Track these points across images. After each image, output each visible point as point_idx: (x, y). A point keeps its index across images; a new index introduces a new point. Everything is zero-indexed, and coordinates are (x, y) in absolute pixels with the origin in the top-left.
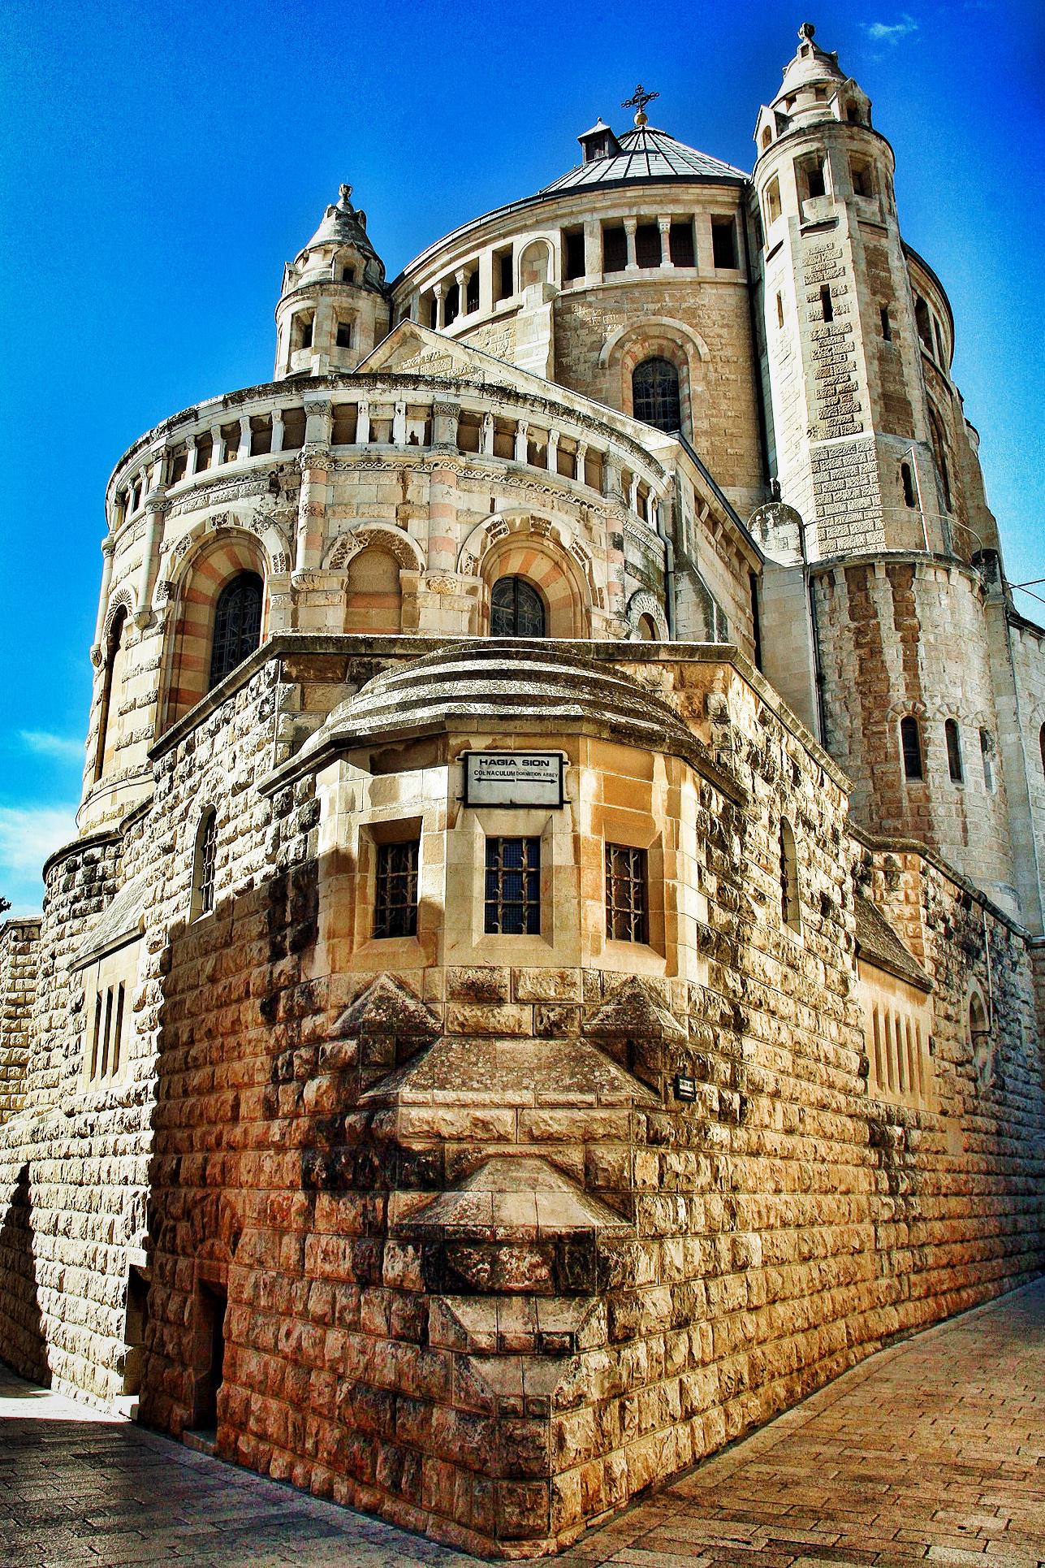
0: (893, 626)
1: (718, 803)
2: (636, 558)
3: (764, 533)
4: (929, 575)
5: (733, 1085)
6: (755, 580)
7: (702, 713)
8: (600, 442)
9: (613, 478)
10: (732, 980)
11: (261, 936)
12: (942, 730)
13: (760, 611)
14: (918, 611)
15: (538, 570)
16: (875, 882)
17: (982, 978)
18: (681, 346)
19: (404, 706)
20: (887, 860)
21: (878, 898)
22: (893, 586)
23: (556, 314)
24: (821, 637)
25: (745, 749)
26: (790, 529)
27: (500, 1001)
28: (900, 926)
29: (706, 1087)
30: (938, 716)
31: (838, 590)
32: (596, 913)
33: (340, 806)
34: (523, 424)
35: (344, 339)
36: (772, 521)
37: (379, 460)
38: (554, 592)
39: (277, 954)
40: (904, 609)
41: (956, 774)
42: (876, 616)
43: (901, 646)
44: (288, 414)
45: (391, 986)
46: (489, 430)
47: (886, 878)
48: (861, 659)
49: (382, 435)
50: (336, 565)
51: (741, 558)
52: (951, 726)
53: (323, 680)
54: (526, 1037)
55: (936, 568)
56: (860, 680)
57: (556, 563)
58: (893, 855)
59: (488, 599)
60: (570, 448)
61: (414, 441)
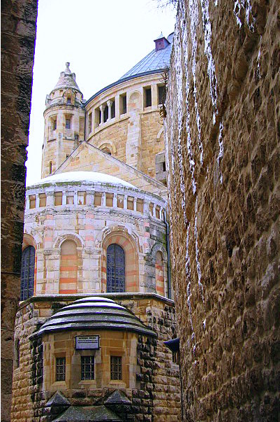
1: (145, 339)
2: (154, 233)
5: (149, 413)
7: (143, 314)
8: (141, 196)
9: (146, 207)
10: (150, 385)
11: (31, 378)
15: (121, 242)
19: (61, 323)
23: (141, 120)
25: (157, 320)
27: (85, 397)
29: (138, 415)
32: (108, 374)
33: (47, 349)
34: (115, 194)
35: (68, 125)
37: (69, 211)
38: (127, 248)
39: (34, 384)
44: (41, 196)
45: (59, 394)
46: (104, 198)
49: (70, 201)
50: (57, 246)
53: (45, 308)
54: (90, 405)
57: (127, 239)
59: (105, 253)
60: (131, 199)
61: (81, 203)
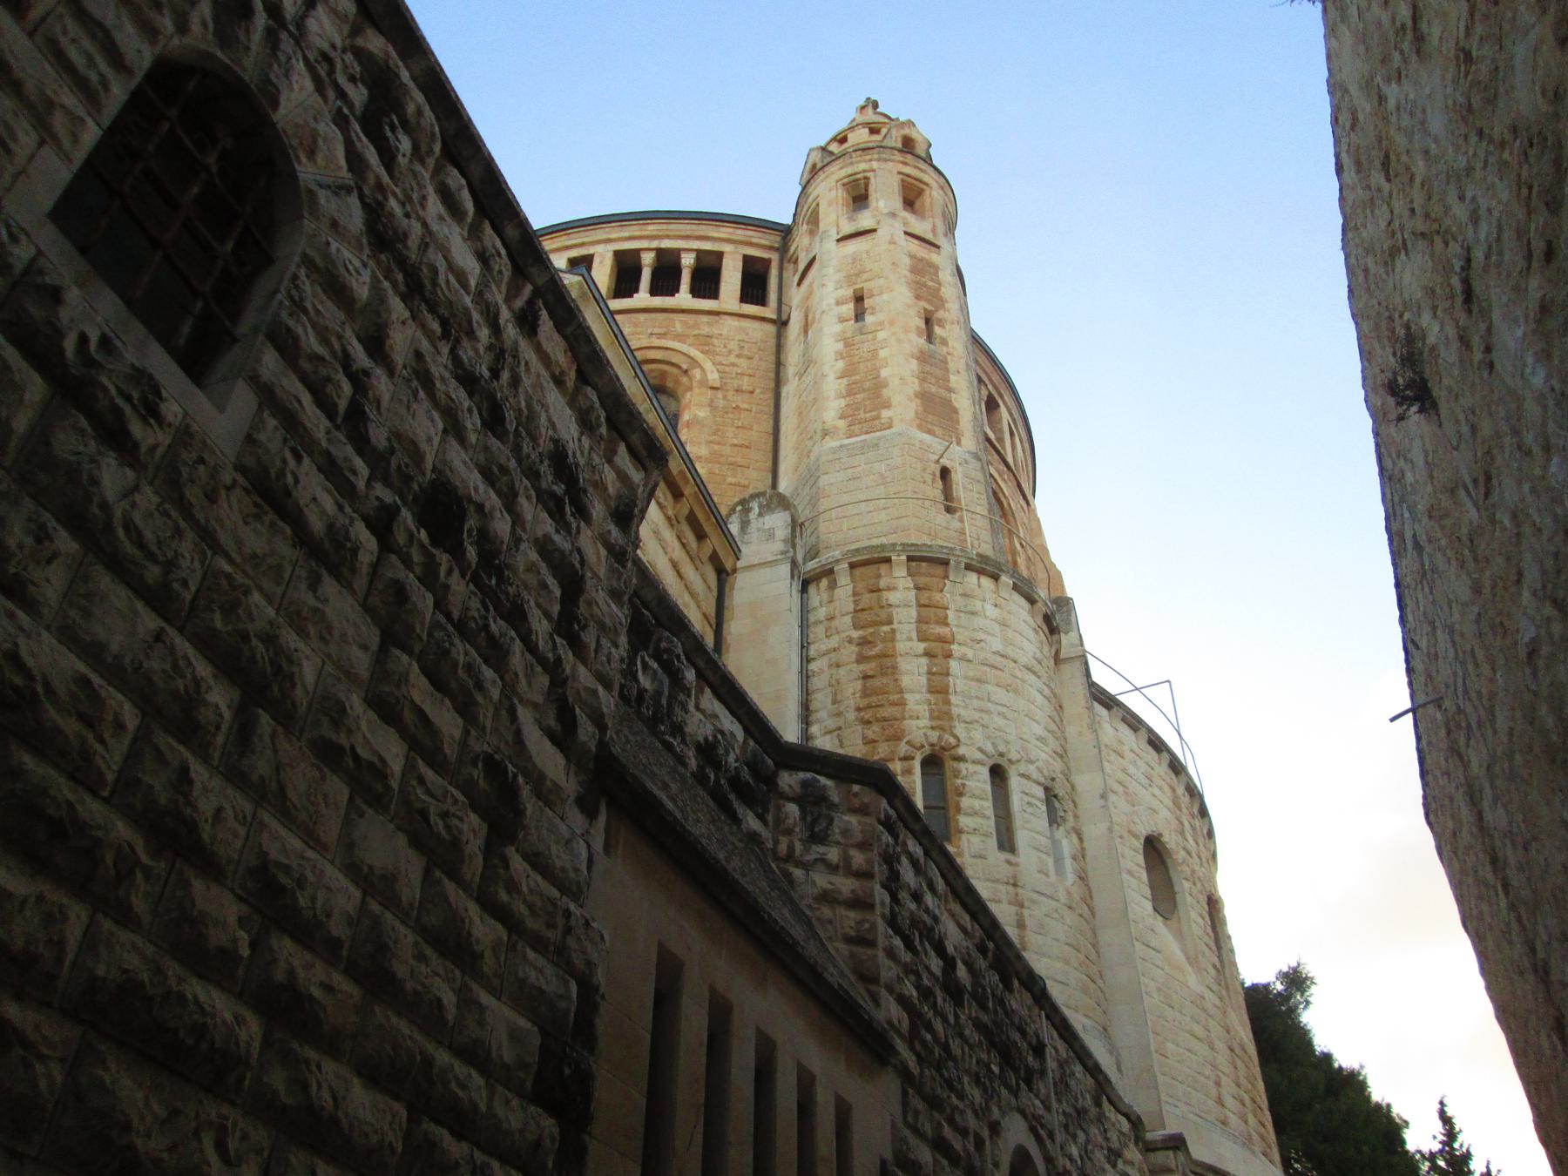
0: (914, 635)
3: (745, 525)
4: (972, 578)
6: (723, 574)
12: (984, 772)
13: (727, 614)
14: (950, 620)
16: (779, 821)
17: (1035, 1126)
18: (686, 372)
20: (805, 784)
21: (783, 848)
22: (918, 588)
24: (812, 653)
26: (778, 521)
28: (826, 912)
30: (979, 756)
31: (839, 592)
36: (756, 510)
40: (930, 613)
41: (1007, 842)
42: (890, 622)
43: (924, 661)
47: (803, 818)
48: (866, 677)
51: (701, 536)
52: (998, 773)
55: (981, 572)
56: (865, 702)
58: (823, 780)
